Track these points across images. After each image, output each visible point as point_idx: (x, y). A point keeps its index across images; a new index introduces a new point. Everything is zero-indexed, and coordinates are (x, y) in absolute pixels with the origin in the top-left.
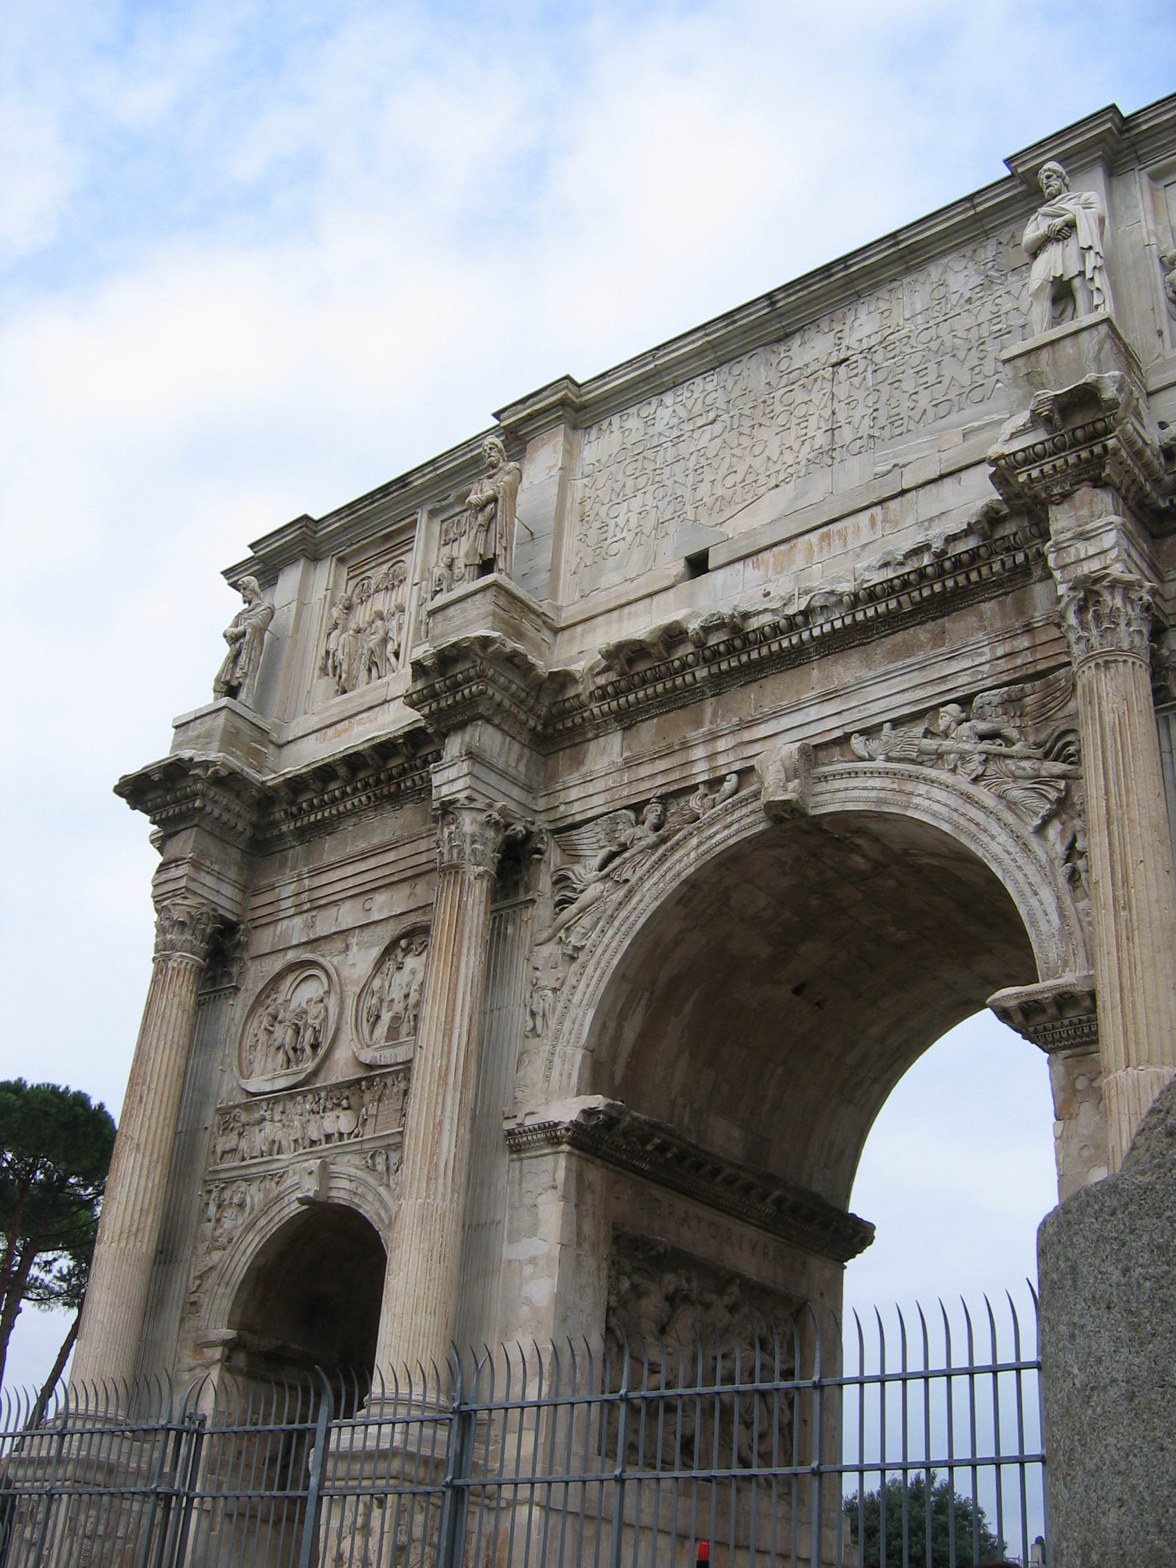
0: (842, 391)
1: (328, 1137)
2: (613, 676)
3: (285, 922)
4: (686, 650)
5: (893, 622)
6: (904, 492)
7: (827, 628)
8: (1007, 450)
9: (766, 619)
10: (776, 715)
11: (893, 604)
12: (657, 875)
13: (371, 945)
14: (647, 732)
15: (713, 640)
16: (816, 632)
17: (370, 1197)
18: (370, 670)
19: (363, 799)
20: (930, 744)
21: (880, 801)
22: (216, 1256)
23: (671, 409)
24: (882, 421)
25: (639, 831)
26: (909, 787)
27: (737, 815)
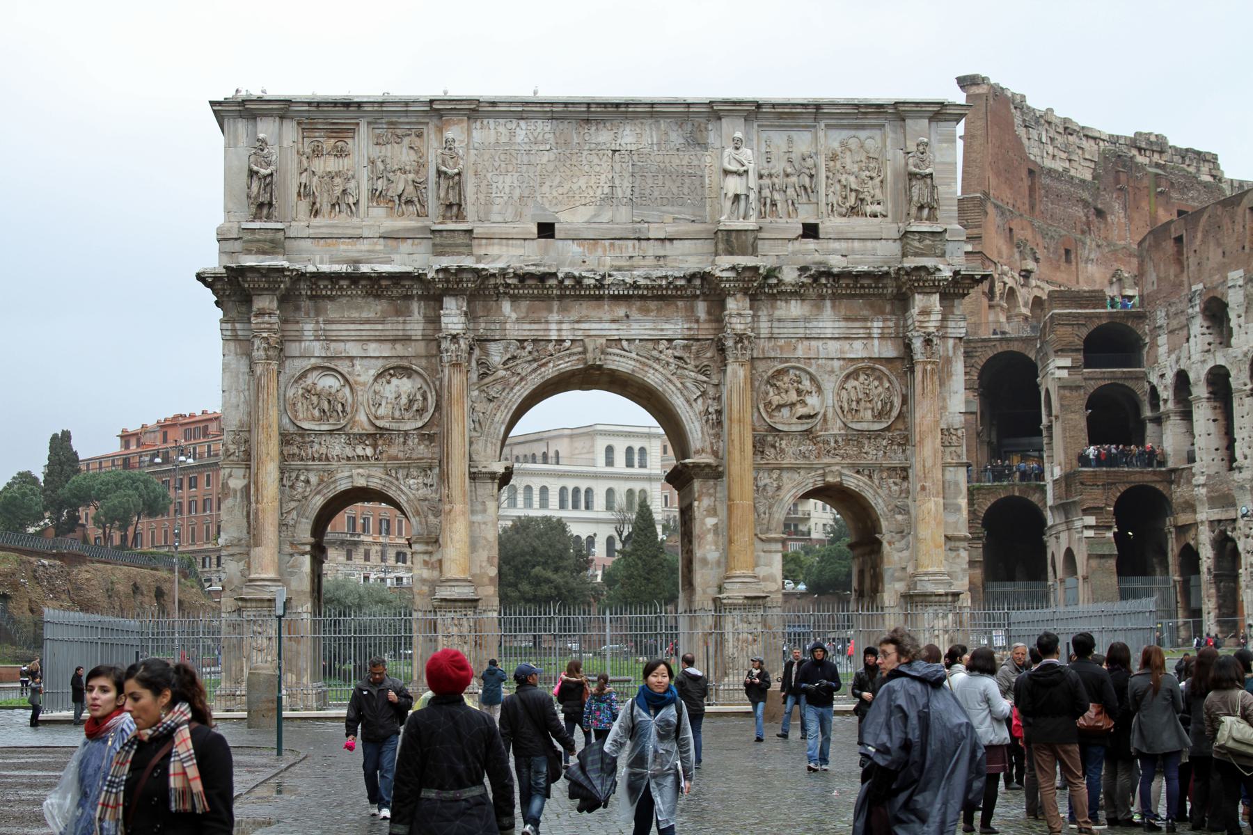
0: (617, 167)
1: (358, 456)
3: (307, 343)
4: (553, 282)
6: (649, 239)
7: (616, 293)
8: (718, 274)
9: (593, 282)
11: (645, 293)
14: (524, 304)
15: (567, 282)
16: (611, 293)
18: (333, 206)
20: (655, 353)
21: (633, 371)
22: (293, 504)
23: (524, 132)
24: (636, 194)
26: (646, 369)
27: (571, 359)
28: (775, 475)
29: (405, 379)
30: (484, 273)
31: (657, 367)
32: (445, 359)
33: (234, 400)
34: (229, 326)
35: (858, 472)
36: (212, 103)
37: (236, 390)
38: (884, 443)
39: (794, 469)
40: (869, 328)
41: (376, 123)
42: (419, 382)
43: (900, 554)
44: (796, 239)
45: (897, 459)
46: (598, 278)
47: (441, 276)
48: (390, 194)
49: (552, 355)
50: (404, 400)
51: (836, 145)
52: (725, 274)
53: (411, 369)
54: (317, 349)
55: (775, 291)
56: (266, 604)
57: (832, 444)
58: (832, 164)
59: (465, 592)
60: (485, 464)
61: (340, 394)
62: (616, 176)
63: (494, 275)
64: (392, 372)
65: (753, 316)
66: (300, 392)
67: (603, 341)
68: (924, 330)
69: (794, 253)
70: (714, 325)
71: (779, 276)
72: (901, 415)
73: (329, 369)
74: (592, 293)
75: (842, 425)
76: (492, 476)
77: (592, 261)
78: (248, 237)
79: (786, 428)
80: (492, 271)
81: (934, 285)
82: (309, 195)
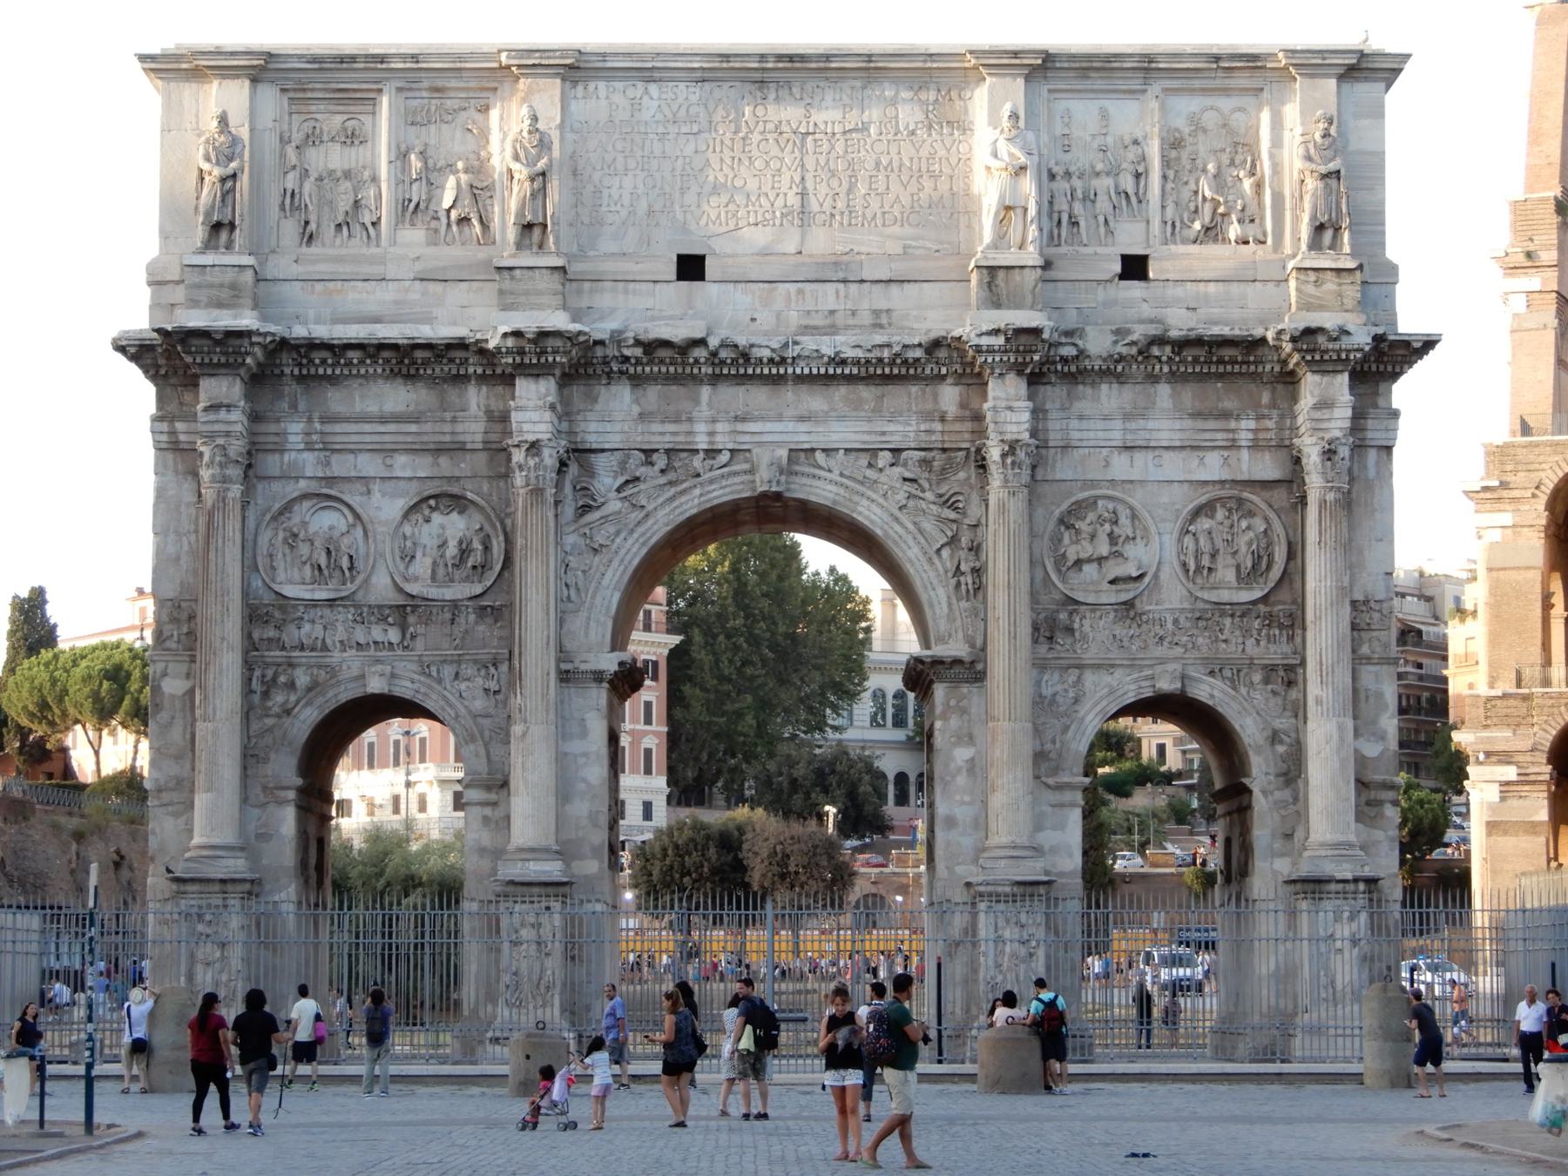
0: (810, 163)
2: (638, 352)
3: (293, 455)
4: (701, 353)
5: (850, 379)
6: (862, 281)
7: (806, 371)
8: (975, 341)
9: (766, 354)
10: (762, 419)
11: (855, 371)
12: (667, 509)
13: (394, 496)
14: (653, 393)
15: (723, 354)
16: (798, 371)
17: (434, 696)
19: (379, 371)
21: (835, 502)
22: (269, 721)
23: (656, 103)
26: (856, 498)
28: (1072, 676)
29: (454, 515)
30: (582, 339)
31: (874, 496)
32: (519, 479)
33: (171, 549)
34: (164, 426)
35: (1212, 673)
36: (143, 58)
37: (178, 533)
38: (1256, 624)
39: (1109, 667)
40: (1233, 431)
41: (410, 89)
42: (477, 520)
43: (1283, 812)
44: (1110, 281)
45: (1277, 652)
46: (776, 346)
47: (510, 342)
48: (432, 207)
49: (698, 475)
50: (452, 550)
51: (1180, 123)
54: (310, 463)
55: (1073, 369)
56: (217, 887)
57: (1170, 626)
58: (1174, 154)
59: (551, 869)
60: (585, 656)
61: (346, 541)
62: (809, 177)
63: (601, 343)
64: (432, 502)
65: (1034, 412)
66: (281, 535)
67: (783, 453)
68: (1321, 434)
69: (1108, 304)
70: (968, 426)
71: (1080, 343)
73: (329, 497)
74: (766, 371)
75: (1185, 592)
76: (598, 676)
77: (766, 319)
78: (195, 278)
79: (1090, 600)
80: (598, 336)
81: (1339, 359)
82: (299, 208)
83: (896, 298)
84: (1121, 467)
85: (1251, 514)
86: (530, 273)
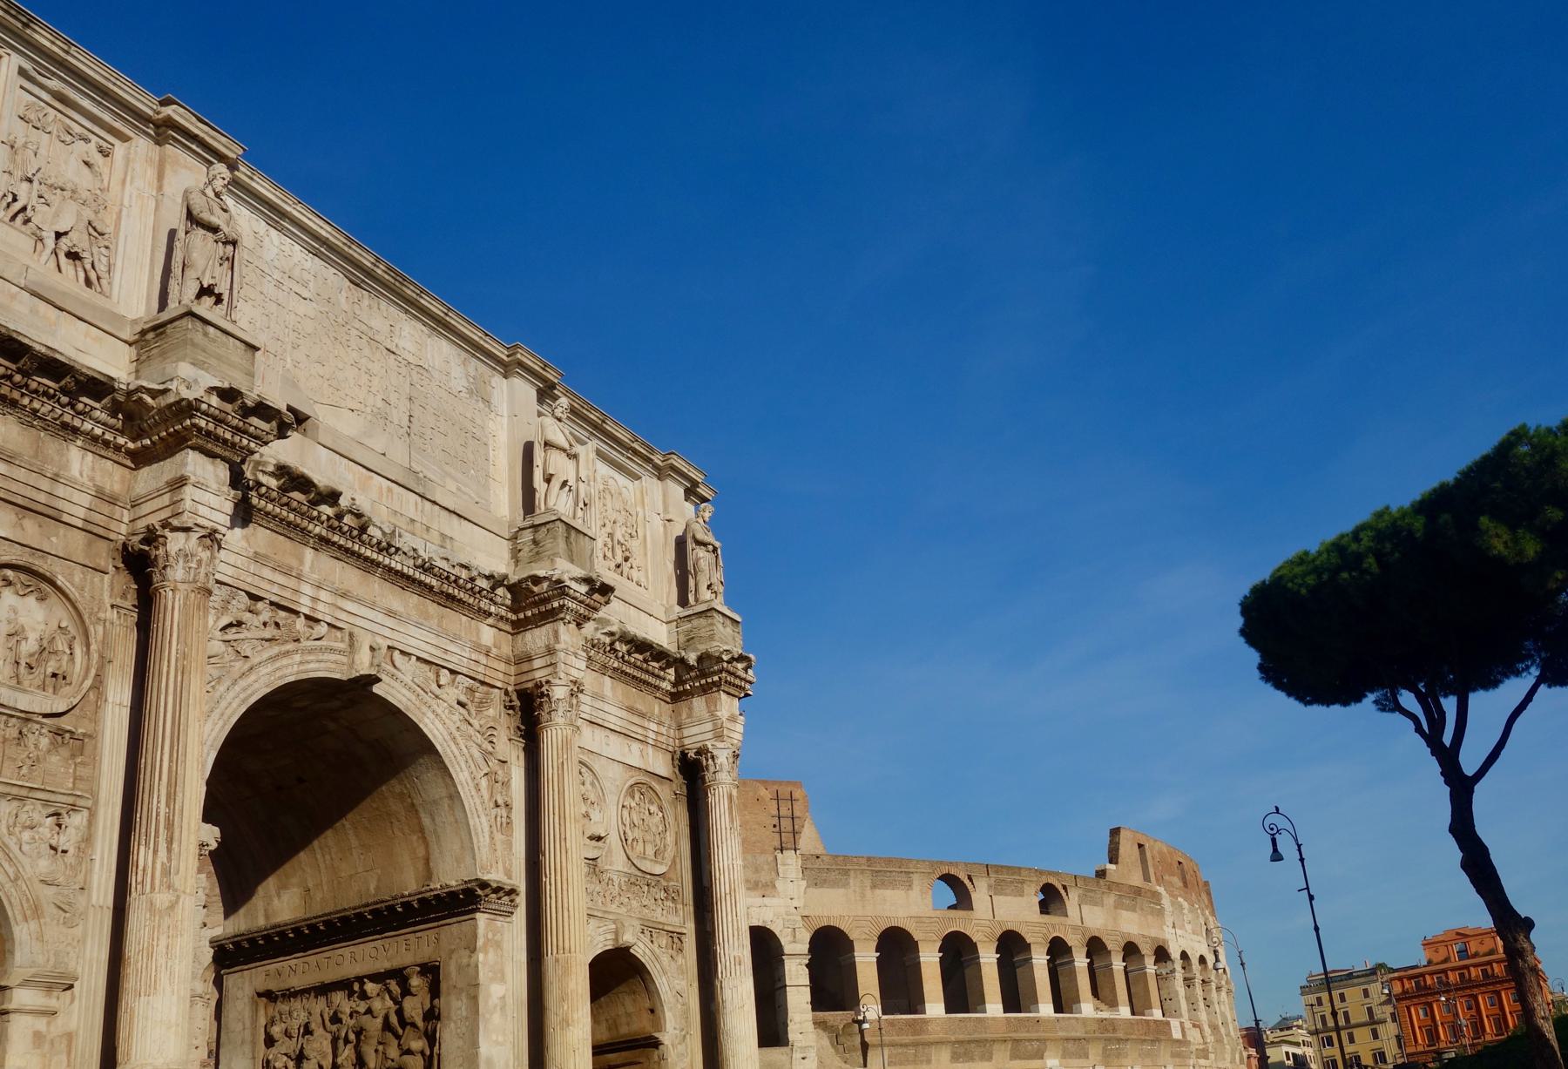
4: (327, 510)
6: (434, 503)
7: (399, 567)
10: (359, 601)
11: (434, 582)
12: (270, 668)
16: (393, 564)
20: (438, 691)
25: (256, 621)
26: (424, 709)
27: (326, 656)
29: (31, 600)
31: (439, 711)
42: (62, 615)
46: (387, 531)
47: (215, 400)
49: (297, 640)
50: (29, 646)
52: (574, 585)
53: (52, 583)
64: (9, 573)
72: (674, 861)
83: (454, 527)
84: (590, 738)
85: (651, 802)
86: (224, 337)
